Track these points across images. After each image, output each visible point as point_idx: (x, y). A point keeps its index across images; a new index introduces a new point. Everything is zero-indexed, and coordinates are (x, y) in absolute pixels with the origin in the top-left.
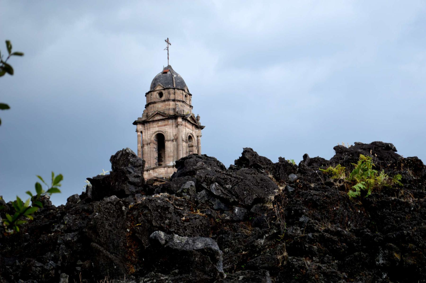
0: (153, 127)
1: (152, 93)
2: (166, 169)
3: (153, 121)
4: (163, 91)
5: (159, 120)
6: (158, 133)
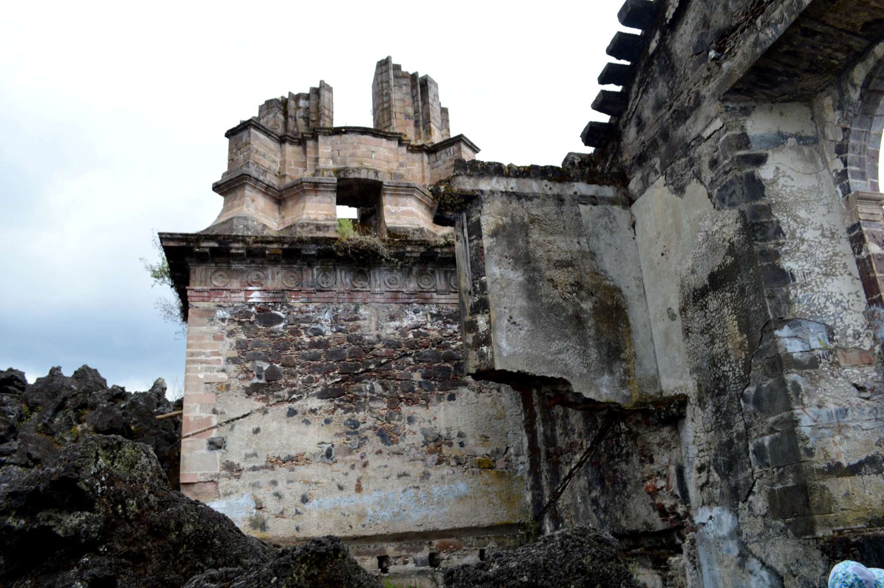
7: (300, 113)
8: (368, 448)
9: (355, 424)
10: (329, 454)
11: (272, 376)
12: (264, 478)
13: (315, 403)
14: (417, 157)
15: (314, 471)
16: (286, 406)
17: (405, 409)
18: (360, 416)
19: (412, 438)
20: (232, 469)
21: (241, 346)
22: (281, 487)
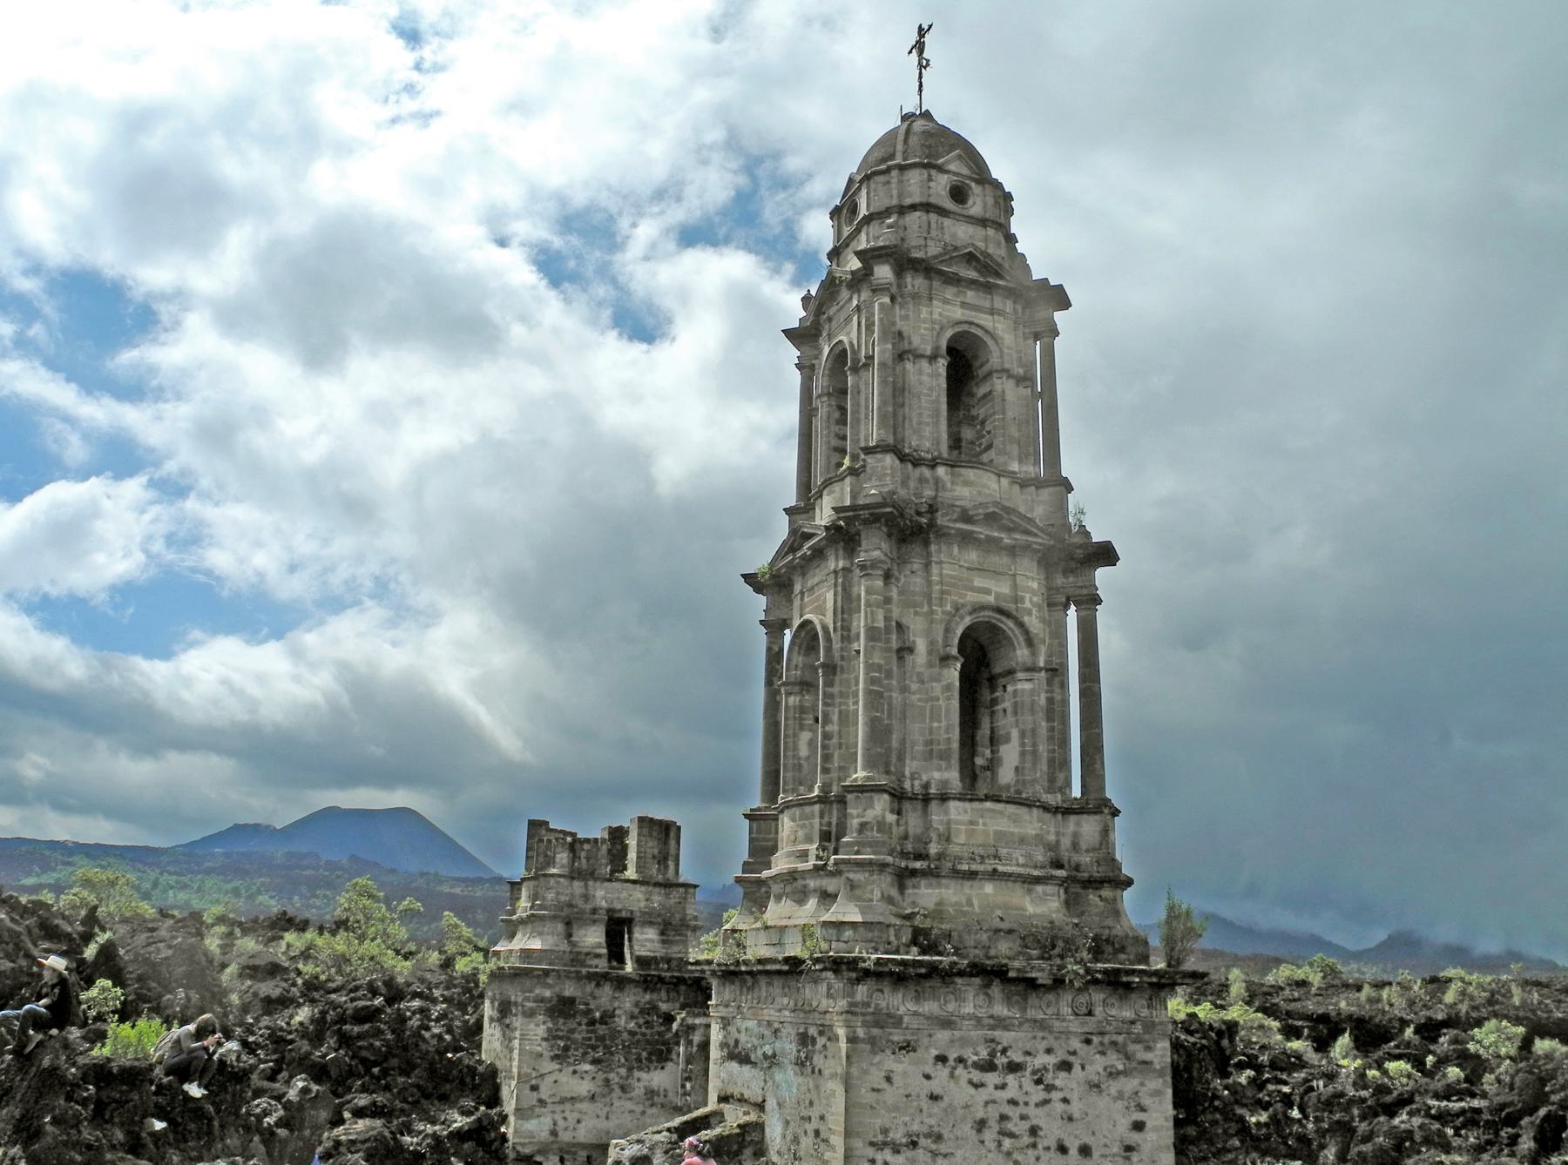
0: (946, 302)
1: (933, 172)
2: (1005, 481)
3: (954, 280)
4: (973, 185)
5: (973, 283)
6: (965, 327)
7: (583, 854)
8: (614, 1095)
9: (607, 1081)
10: (593, 1097)
11: (566, 1049)
12: (558, 1108)
13: (587, 1067)
14: (657, 890)
15: (585, 1106)
16: (571, 1069)
17: (636, 1074)
18: (612, 1076)
19: (638, 1090)
20: (542, 1102)
21: (549, 1030)
22: (567, 1114)
